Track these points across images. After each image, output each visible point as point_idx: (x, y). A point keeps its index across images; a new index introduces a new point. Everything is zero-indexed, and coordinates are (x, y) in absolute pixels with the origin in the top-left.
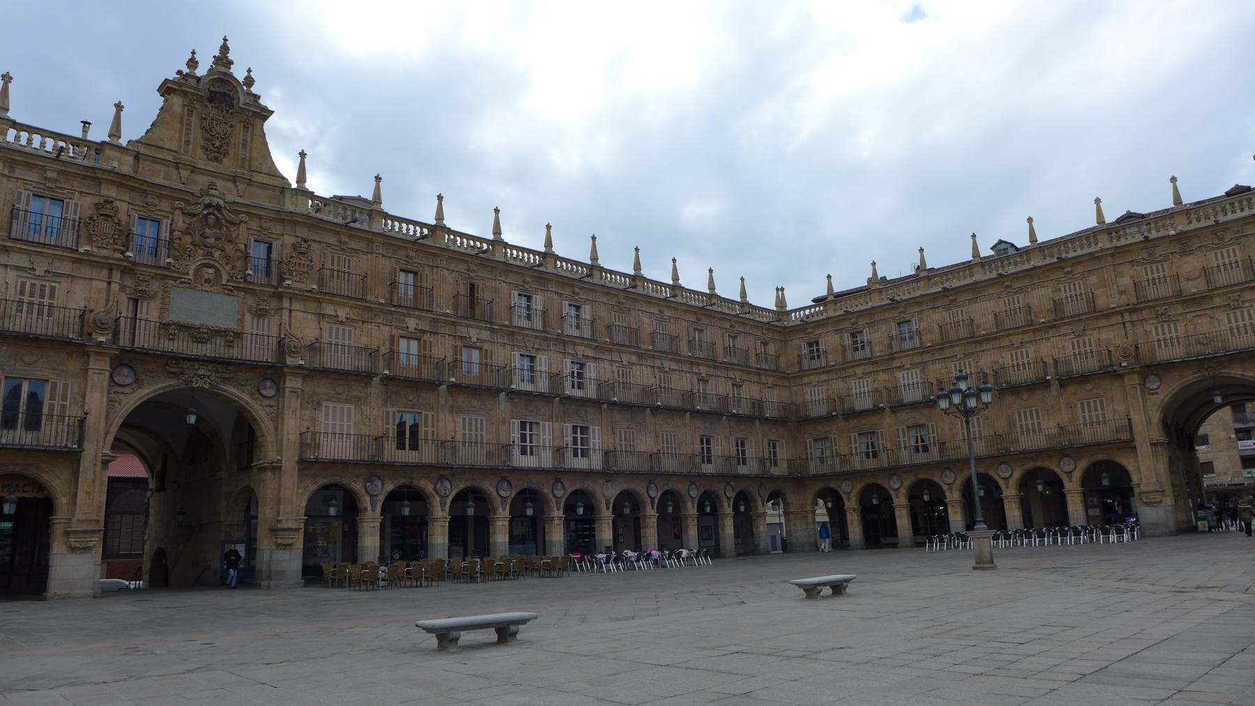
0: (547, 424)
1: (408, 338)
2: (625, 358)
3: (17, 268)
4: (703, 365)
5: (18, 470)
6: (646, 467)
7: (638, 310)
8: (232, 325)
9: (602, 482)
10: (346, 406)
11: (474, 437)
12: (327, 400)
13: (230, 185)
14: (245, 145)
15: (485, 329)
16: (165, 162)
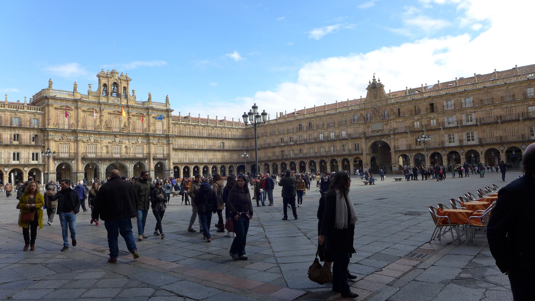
0: (457, 134)
1: (417, 121)
2: (488, 109)
3: (353, 128)
4: (530, 101)
5: (357, 157)
6: (499, 141)
7: (495, 91)
8: (382, 128)
9: (478, 147)
10: (404, 139)
11: (434, 141)
12: (400, 138)
13: (378, 102)
14: (379, 94)
15: (435, 114)
16: (368, 103)
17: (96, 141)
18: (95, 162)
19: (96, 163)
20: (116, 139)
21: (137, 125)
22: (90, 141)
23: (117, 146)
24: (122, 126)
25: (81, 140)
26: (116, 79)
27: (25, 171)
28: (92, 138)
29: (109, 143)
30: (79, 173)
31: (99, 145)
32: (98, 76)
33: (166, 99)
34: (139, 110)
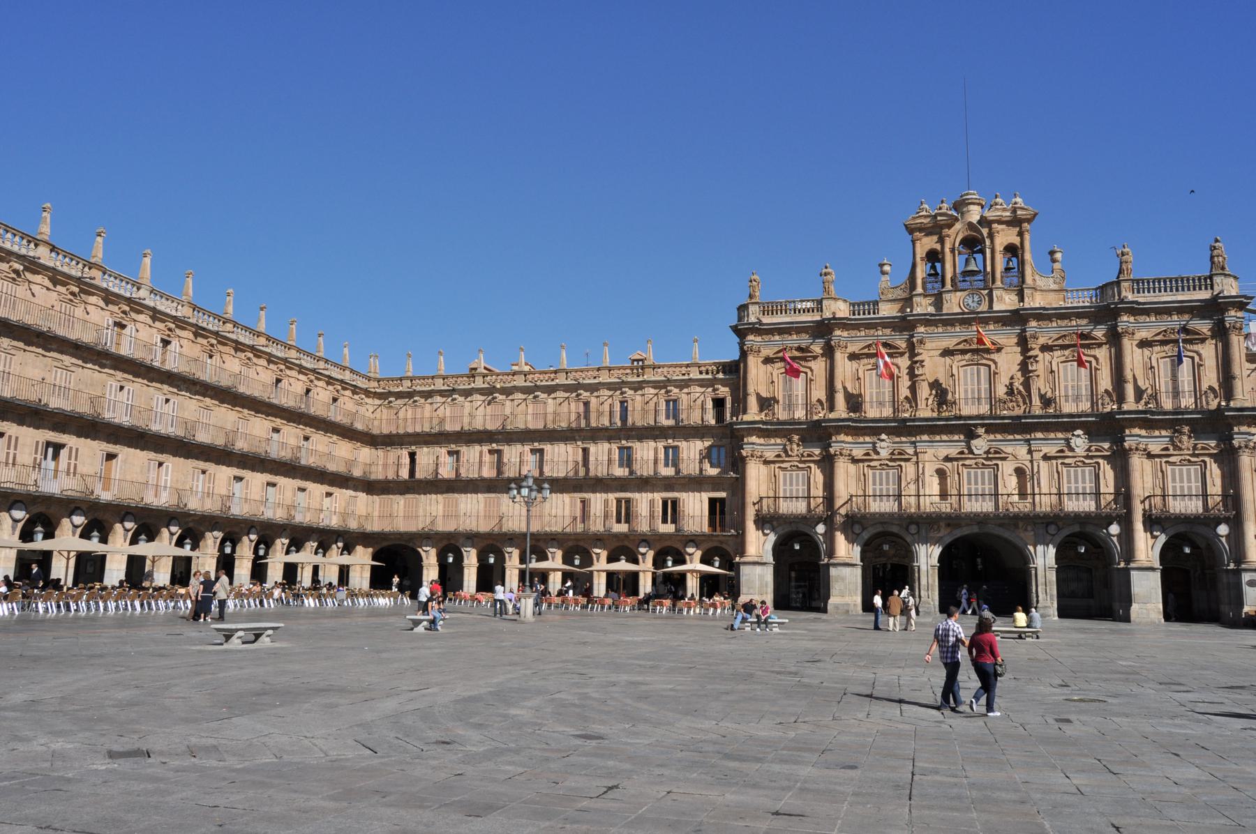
17: (898, 457)
18: (895, 529)
19: (903, 533)
20: (974, 442)
21: (1066, 380)
22: (875, 457)
23: (979, 471)
24: (1001, 391)
25: (841, 454)
26: (970, 225)
27: (690, 555)
28: (883, 444)
29: (947, 459)
30: (835, 565)
31: (909, 469)
32: (911, 230)
33: (1212, 257)
34: (1074, 323)
